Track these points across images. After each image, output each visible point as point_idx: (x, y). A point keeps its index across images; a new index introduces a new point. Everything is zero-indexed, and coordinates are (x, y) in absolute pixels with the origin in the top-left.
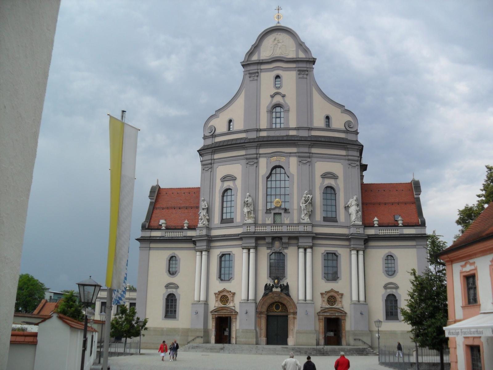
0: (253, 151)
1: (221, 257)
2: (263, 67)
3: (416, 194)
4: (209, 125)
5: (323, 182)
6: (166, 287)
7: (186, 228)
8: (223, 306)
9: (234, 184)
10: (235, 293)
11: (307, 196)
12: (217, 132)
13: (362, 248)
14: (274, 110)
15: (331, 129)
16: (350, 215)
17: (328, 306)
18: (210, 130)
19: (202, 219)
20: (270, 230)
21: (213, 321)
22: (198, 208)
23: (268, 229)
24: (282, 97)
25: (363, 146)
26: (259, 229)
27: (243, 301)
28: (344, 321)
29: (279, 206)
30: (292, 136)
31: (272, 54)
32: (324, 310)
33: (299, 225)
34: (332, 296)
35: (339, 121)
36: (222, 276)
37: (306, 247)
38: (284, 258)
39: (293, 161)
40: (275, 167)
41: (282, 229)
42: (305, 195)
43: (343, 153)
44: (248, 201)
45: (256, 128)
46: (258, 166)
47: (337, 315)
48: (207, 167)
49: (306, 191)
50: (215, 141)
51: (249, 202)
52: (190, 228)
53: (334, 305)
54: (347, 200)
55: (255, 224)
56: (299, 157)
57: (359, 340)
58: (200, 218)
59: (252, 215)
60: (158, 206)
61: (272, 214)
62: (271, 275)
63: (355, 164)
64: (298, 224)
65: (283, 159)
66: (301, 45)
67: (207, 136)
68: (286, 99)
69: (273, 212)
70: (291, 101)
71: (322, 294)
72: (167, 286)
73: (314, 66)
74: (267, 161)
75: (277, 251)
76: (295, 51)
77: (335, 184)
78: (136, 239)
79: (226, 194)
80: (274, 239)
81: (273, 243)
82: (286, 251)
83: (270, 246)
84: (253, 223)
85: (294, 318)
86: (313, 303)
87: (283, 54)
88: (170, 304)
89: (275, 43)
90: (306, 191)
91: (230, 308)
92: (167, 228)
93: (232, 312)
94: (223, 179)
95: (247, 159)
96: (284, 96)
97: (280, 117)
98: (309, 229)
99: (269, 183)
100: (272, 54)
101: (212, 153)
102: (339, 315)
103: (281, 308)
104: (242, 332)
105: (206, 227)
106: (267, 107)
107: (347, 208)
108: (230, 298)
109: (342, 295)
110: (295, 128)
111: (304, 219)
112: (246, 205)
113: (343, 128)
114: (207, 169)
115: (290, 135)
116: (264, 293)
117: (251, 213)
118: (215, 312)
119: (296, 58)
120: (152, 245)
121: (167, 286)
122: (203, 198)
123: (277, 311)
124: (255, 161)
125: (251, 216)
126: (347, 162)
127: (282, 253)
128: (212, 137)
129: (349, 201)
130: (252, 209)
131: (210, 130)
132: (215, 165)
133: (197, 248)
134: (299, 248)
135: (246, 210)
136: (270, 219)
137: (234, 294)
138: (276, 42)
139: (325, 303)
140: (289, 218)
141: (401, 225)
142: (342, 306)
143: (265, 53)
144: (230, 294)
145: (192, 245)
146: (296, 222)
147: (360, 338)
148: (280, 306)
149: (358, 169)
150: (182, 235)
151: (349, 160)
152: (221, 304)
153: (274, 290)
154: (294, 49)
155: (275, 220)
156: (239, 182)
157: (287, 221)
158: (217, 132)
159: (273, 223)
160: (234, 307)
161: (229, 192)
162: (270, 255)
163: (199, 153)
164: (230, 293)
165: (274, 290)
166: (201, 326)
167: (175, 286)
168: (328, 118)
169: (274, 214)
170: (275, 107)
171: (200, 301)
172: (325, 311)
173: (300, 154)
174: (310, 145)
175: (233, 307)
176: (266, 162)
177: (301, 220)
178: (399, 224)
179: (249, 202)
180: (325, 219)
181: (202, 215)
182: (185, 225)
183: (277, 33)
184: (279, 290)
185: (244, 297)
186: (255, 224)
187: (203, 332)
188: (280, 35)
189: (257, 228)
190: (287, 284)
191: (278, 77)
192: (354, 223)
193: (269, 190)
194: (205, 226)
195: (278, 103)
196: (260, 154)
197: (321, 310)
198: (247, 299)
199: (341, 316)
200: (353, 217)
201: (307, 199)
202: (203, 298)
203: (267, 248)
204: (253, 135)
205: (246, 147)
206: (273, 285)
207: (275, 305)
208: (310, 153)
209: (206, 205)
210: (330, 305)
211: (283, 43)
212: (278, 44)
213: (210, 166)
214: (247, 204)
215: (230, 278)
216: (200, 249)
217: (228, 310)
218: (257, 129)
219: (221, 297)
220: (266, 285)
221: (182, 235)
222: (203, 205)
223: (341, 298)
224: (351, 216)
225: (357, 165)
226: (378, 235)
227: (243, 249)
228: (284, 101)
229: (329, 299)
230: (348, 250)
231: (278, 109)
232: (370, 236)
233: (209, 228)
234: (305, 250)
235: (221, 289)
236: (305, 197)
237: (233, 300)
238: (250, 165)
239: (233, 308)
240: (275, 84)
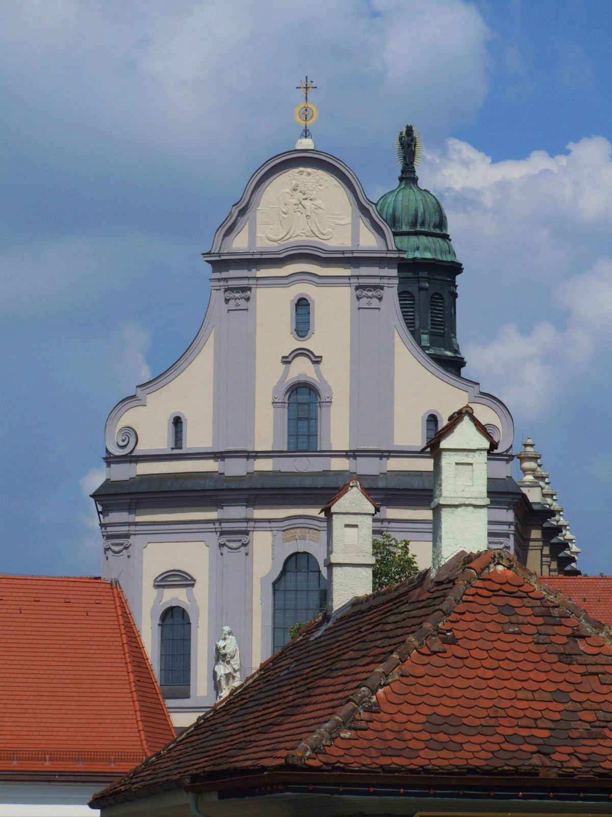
2: (263, 272)
4: (121, 424)
24: (314, 362)
44: (226, 648)
63: (501, 543)
68: (322, 366)
89: (295, 201)
96: (318, 362)
101: (130, 505)
106: (275, 390)
115: (332, 469)
117: (234, 677)
131: (123, 441)
138: (298, 195)
154: (349, 220)
176: (270, 543)
183: (301, 169)
188: (309, 174)
191: (302, 304)
195: (302, 379)
204: (235, 468)
212: (304, 202)
214: (225, 655)
228: (319, 374)
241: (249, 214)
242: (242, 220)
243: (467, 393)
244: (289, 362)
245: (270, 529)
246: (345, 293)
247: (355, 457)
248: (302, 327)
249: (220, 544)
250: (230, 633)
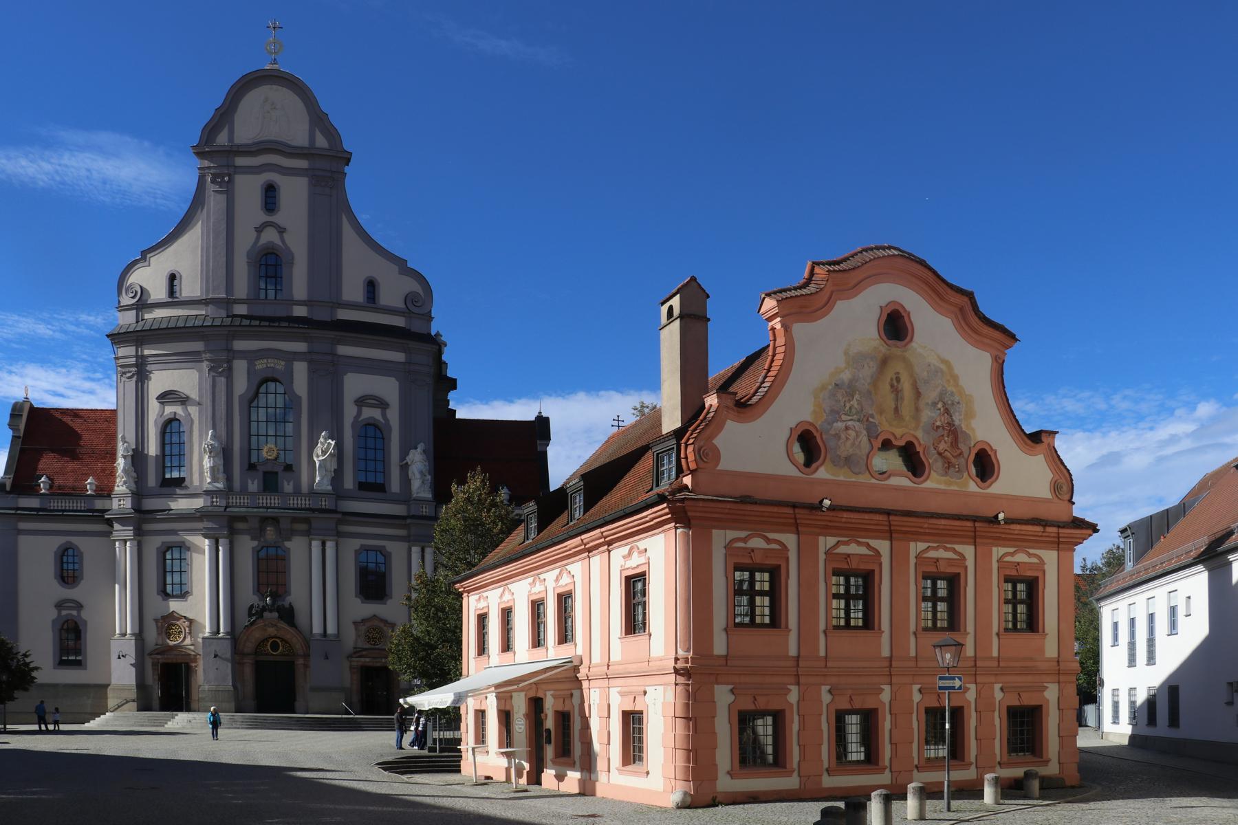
2: (240, 161)
5: (359, 413)
21: (154, 670)
32: (357, 652)
35: (393, 292)
39: (300, 370)
40: (265, 381)
43: (399, 357)
48: (129, 372)
61: (261, 475)
62: (259, 589)
66: (319, 119)
70: (297, 244)
71: (355, 623)
72: (60, 605)
73: (347, 169)
77: (382, 420)
79: (168, 430)
80: (264, 520)
82: (287, 544)
83: (258, 534)
91: (186, 649)
103: (281, 648)
118: (157, 654)
143: (246, 128)
162: (258, 552)
180: (363, 486)
197: (355, 653)
200: (416, 484)
239: (192, 648)
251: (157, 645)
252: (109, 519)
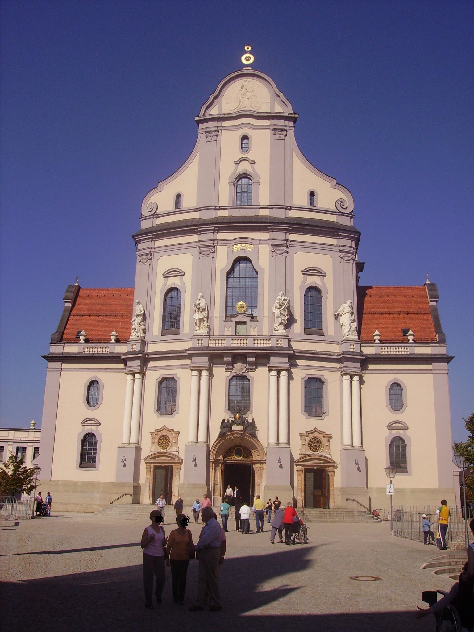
0: (209, 236)
1: (161, 383)
2: (225, 124)
3: (431, 301)
6: (82, 423)
7: (113, 341)
8: (162, 450)
9: (182, 281)
10: (179, 432)
11: (283, 298)
12: (160, 211)
13: (358, 372)
14: (239, 182)
15: (316, 209)
16: (342, 326)
17: (310, 453)
18: (151, 209)
19: (136, 329)
20: (229, 345)
21: (147, 472)
22: (131, 315)
23: (227, 343)
24: (251, 164)
25: (360, 233)
26: (214, 343)
27: (190, 444)
28: (332, 473)
29: (242, 311)
30: (263, 217)
31: (238, 106)
32: (305, 458)
33: (270, 338)
34: (315, 438)
36: (162, 409)
37: (279, 368)
38: (249, 384)
39: (265, 251)
41: (246, 343)
42: (279, 297)
44: (200, 305)
45: (214, 205)
46: (215, 257)
47: (322, 464)
49: (281, 292)
50: (157, 224)
51: (201, 305)
52: (118, 341)
53: (317, 451)
54: (337, 306)
55: (209, 335)
56: (272, 245)
57: (353, 500)
58: (133, 327)
59: (205, 323)
60: (75, 311)
61: (233, 324)
64: (270, 336)
65: (250, 247)
67: (146, 217)
69: (234, 320)
71: (301, 435)
72: (84, 423)
74: (227, 251)
75: (239, 374)
76: (270, 103)
77: (321, 284)
78: (42, 356)
79: (170, 295)
81: (232, 364)
84: (206, 334)
85: (262, 469)
86: (289, 447)
87: (253, 108)
88: (87, 448)
89: (242, 93)
90: (281, 292)
92: (87, 341)
93: (174, 459)
94: (166, 274)
95: (200, 247)
96: (253, 164)
97: (247, 192)
98: (284, 343)
99: (230, 280)
100: (238, 106)
102: (325, 464)
104: (187, 487)
105: (141, 340)
106: (230, 177)
107: (337, 317)
108: (173, 440)
109: (330, 437)
110: (268, 206)
111: (277, 330)
112: (197, 309)
113: (333, 209)
114: (144, 261)
116: (220, 432)
117: (204, 321)
119: (271, 113)
120: (65, 365)
121: (84, 423)
122: (137, 301)
123: (237, 458)
124: (212, 249)
125: (203, 325)
126: (338, 254)
127: (245, 376)
128: (153, 218)
129: (339, 308)
130: (206, 315)
131: (151, 209)
132: (155, 256)
133: (127, 369)
134: (270, 370)
135: (197, 316)
136: (230, 329)
137: (178, 433)
138: (244, 91)
139: (306, 447)
140: (256, 328)
141: (411, 341)
142: (330, 453)
144: (172, 434)
145: (121, 366)
146: (266, 333)
147: (356, 499)
148: (243, 450)
149: (353, 264)
150: (108, 351)
151: (341, 251)
152: (159, 448)
153: (235, 427)
154: (269, 101)
155: (237, 331)
156: (188, 279)
157: (254, 333)
158: (160, 211)
159: (234, 335)
160: (178, 452)
161: (174, 293)
162: (230, 380)
163: (135, 240)
164: (173, 433)
165: (235, 427)
166: (130, 479)
167: (95, 422)
168: (312, 194)
169: (237, 323)
170: (241, 179)
171: (129, 444)
172: (305, 459)
173: (273, 241)
174: (287, 230)
175: (176, 452)
177: (274, 331)
178: (408, 341)
179: (201, 305)
181: (135, 323)
182: (112, 337)
184: (241, 428)
185: (192, 437)
186: (209, 335)
187: (132, 487)
189: (212, 342)
190: (253, 420)
191: (245, 137)
192: (347, 337)
193: (230, 290)
194: (140, 339)
195: (244, 172)
196: (218, 241)
197: (301, 458)
198: (195, 440)
199: (329, 466)
201: (282, 302)
202: (134, 440)
203: (226, 369)
204: (209, 215)
205: (200, 231)
206: (232, 421)
207: (235, 450)
208: (287, 241)
209: (142, 309)
210: (313, 451)
211: (253, 93)
213: (149, 257)
214: (199, 308)
215: (172, 412)
216: (132, 371)
217: (169, 457)
218: (216, 207)
219: (160, 438)
220: (224, 421)
221: (108, 351)
222: (138, 309)
223: (329, 441)
224: (343, 327)
225: (352, 259)
226: (380, 354)
227: (192, 370)
229: (312, 442)
230: (339, 374)
231: (244, 181)
232: (369, 356)
233: (144, 343)
234: (279, 372)
235: (159, 427)
236: (280, 300)
237: (176, 443)
238: (204, 256)
239: (177, 454)
240: (242, 147)
241: (218, 100)
242: (216, 101)
243: (330, 183)
244: (238, 164)
245: (226, 245)
246: (268, 134)
247: (272, 208)
248: (244, 149)
249: (199, 253)
250: (202, 297)
251: (150, 452)
252: (123, 359)
